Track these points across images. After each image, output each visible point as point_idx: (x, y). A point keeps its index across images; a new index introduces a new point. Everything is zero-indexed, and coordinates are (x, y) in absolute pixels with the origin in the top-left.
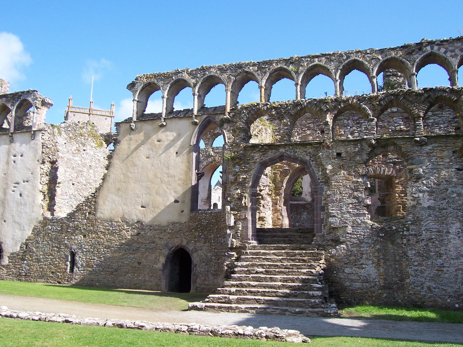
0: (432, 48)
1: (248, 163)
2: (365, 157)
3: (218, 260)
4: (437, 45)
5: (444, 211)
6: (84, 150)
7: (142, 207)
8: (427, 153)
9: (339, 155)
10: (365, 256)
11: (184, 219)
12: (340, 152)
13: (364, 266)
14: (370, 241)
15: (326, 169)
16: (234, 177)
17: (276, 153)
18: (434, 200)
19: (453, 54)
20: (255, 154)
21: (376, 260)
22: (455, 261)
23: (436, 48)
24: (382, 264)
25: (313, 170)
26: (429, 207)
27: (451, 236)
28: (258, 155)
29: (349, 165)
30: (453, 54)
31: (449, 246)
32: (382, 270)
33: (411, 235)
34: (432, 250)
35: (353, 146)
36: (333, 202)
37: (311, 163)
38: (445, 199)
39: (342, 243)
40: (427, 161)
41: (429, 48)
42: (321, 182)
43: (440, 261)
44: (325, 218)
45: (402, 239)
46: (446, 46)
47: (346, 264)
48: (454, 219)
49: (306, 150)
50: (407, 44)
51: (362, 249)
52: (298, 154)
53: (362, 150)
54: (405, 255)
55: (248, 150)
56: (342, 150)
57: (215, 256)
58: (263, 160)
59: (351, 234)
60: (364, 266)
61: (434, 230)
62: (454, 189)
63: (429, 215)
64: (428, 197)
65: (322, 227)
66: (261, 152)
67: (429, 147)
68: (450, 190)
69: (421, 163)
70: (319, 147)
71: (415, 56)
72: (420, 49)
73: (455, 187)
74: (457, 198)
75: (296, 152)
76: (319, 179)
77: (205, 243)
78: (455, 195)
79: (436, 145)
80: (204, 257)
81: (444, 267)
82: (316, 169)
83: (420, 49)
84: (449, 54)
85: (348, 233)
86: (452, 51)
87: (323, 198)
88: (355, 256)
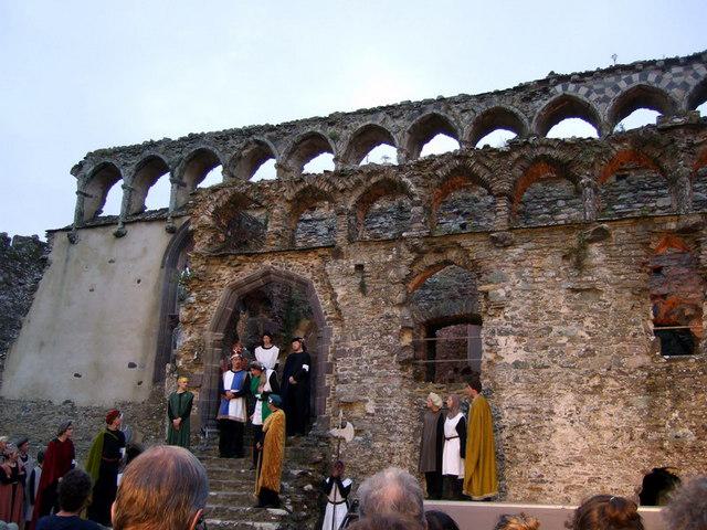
0: (565, 88)
1: (212, 287)
2: (404, 271)
4: (575, 82)
5: (544, 370)
6: (21, 284)
7: (76, 375)
8: (515, 261)
9: (360, 267)
11: (143, 396)
14: (406, 430)
18: (527, 350)
19: (602, 96)
22: (566, 470)
23: (571, 87)
26: (516, 364)
27: (556, 420)
30: (602, 96)
31: (553, 440)
34: (520, 447)
37: (315, 285)
38: (546, 348)
40: (513, 275)
41: (559, 88)
42: (329, 319)
43: (535, 470)
46: (590, 83)
48: (563, 386)
50: (523, 82)
56: (364, 259)
59: (373, 415)
61: (524, 408)
62: (563, 329)
63: (517, 379)
64: (515, 344)
67: (519, 250)
68: (556, 329)
69: (504, 279)
71: (537, 103)
72: (546, 91)
73: (564, 324)
74: (568, 345)
78: (565, 340)
79: (532, 245)
81: (543, 482)
83: (546, 91)
84: (594, 96)
85: (368, 414)
86: (598, 92)
88: (379, 458)
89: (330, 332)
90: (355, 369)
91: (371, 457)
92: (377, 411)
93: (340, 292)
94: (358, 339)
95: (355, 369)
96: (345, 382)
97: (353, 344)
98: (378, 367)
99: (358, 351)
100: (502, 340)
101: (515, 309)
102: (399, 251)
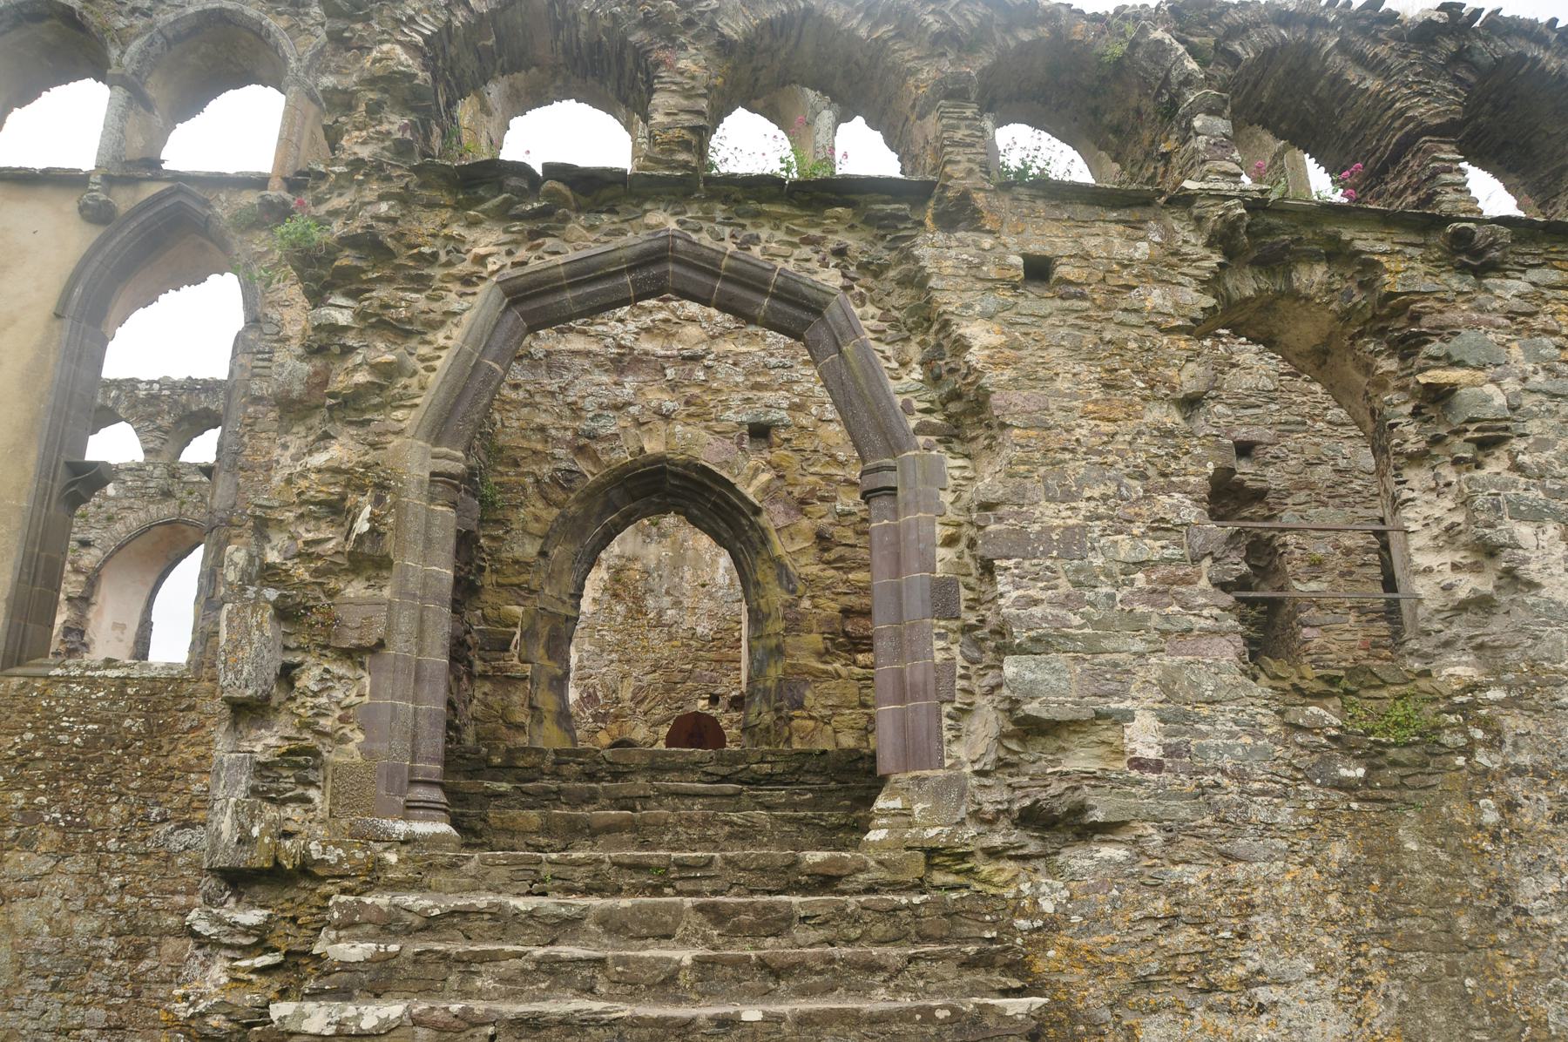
3: (139, 954)
10: (1264, 925)
12: (1048, 251)
13: (1263, 995)
14: (1284, 815)
15: (962, 345)
16: (307, 368)
17: (622, 233)
20: (470, 235)
21: (1335, 948)
24: (1377, 976)
25: (864, 349)
28: (493, 238)
29: (1107, 336)
32: (1380, 1014)
33: (1519, 771)
35: (1121, 228)
36: (1021, 544)
37: (858, 312)
39: (1107, 830)
40: (1516, 351)
42: (922, 429)
44: (960, 661)
45: (1472, 799)
47: (1146, 983)
49: (815, 232)
51: (1238, 871)
52: (764, 251)
53: (1175, 260)
54: (1505, 902)
55: (431, 205)
57: (118, 934)
58: (527, 270)
59: (1158, 766)
60: (1263, 995)
65: (946, 722)
66: (521, 217)
70: (905, 218)
75: (756, 240)
76: (907, 409)
77: (63, 852)
80: (45, 937)
82: (882, 347)
85: (1138, 764)
87: (941, 532)
88: (1199, 923)
89: (935, 475)
90: (1066, 602)
91: (1171, 922)
92: (1172, 752)
93: (981, 337)
94: (1069, 496)
95: (1066, 602)
96: (1040, 645)
97: (1052, 516)
98: (1153, 595)
99: (1072, 542)
100: (1524, 531)
101: (1542, 444)
102: (1169, 233)
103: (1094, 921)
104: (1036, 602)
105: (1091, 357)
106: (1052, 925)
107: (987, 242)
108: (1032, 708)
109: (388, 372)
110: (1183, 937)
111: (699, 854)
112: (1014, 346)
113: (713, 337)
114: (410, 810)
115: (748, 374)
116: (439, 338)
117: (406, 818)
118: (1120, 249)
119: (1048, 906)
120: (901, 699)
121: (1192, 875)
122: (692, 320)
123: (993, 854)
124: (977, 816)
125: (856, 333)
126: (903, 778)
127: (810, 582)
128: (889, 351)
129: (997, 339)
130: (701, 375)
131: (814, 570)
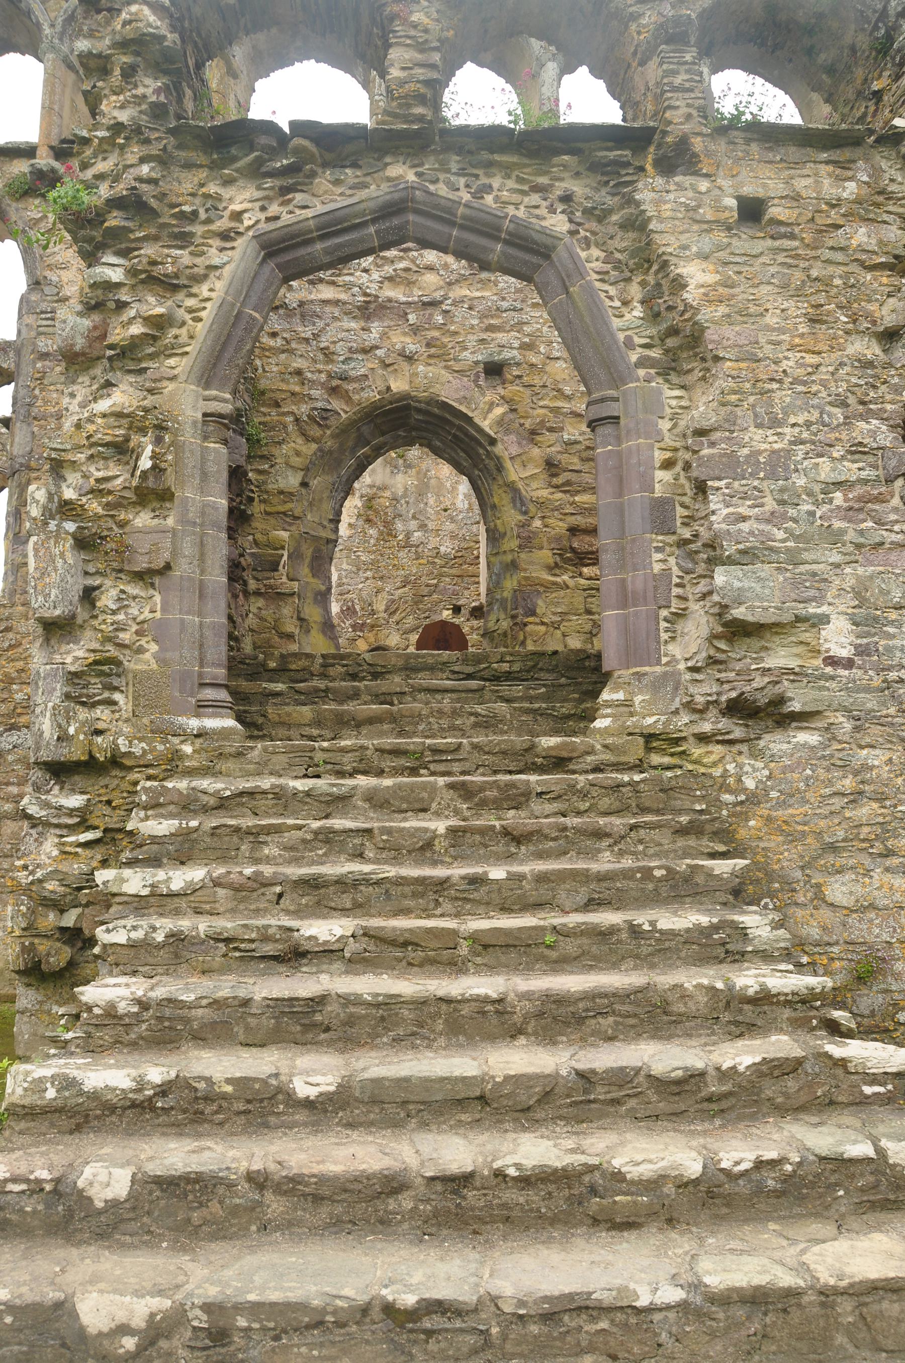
12: (761, 193)
15: (679, 284)
16: (86, 323)
17: (365, 186)
20: (226, 193)
25: (589, 290)
28: (247, 195)
29: (814, 273)
35: (830, 168)
37: (583, 255)
39: (802, 718)
42: (642, 362)
44: (676, 571)
47: (833, 848)
49: (543, 180)
52: (497, 199)
53: (880, 199)
55: (188, 166)
58: (279, 224)
59: (849, 664)
65: (663, 625)
66: (271, 174)
70: (628, 164)
75: (489, 189)
76: (629, 344)
82: (606, 287)
85: (832, 661)
87: (659, 456)
88: (881, 799)
89: (654, 406)
90: (771, 519)
91: (856, 797)
92: (862, 651)
94: (775, 423)
95: (771, 519)
96: (747, 557)
98: (850, 512)
102: (876, 172)
103: (790, 796)
104: (744, 519)
105: (798, 294)
106: (754, 799)
107: (704, 185)
108: (739, 612)
109: (160, 324)
110: (866, 810)
111: (449, 740)
112: (728, 284)
113: (450, 284)
114: (201, 708)
115: (483, 317)
116: (204, 290)
117: (198, 716)
118: (829, 189)
119: (750, 784)
120: (624, 605)
121: (876, 758)
122: (430, 268)
123: (703, 738)
124: (689, 706)
125: (582, 275)
126: (625, 674)
127: (541, 504)
128: (612, 291)
129: (711, 278)
130: (440, 319)
131: (544, 493)
